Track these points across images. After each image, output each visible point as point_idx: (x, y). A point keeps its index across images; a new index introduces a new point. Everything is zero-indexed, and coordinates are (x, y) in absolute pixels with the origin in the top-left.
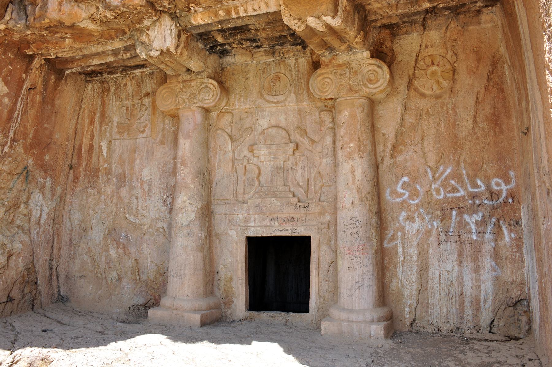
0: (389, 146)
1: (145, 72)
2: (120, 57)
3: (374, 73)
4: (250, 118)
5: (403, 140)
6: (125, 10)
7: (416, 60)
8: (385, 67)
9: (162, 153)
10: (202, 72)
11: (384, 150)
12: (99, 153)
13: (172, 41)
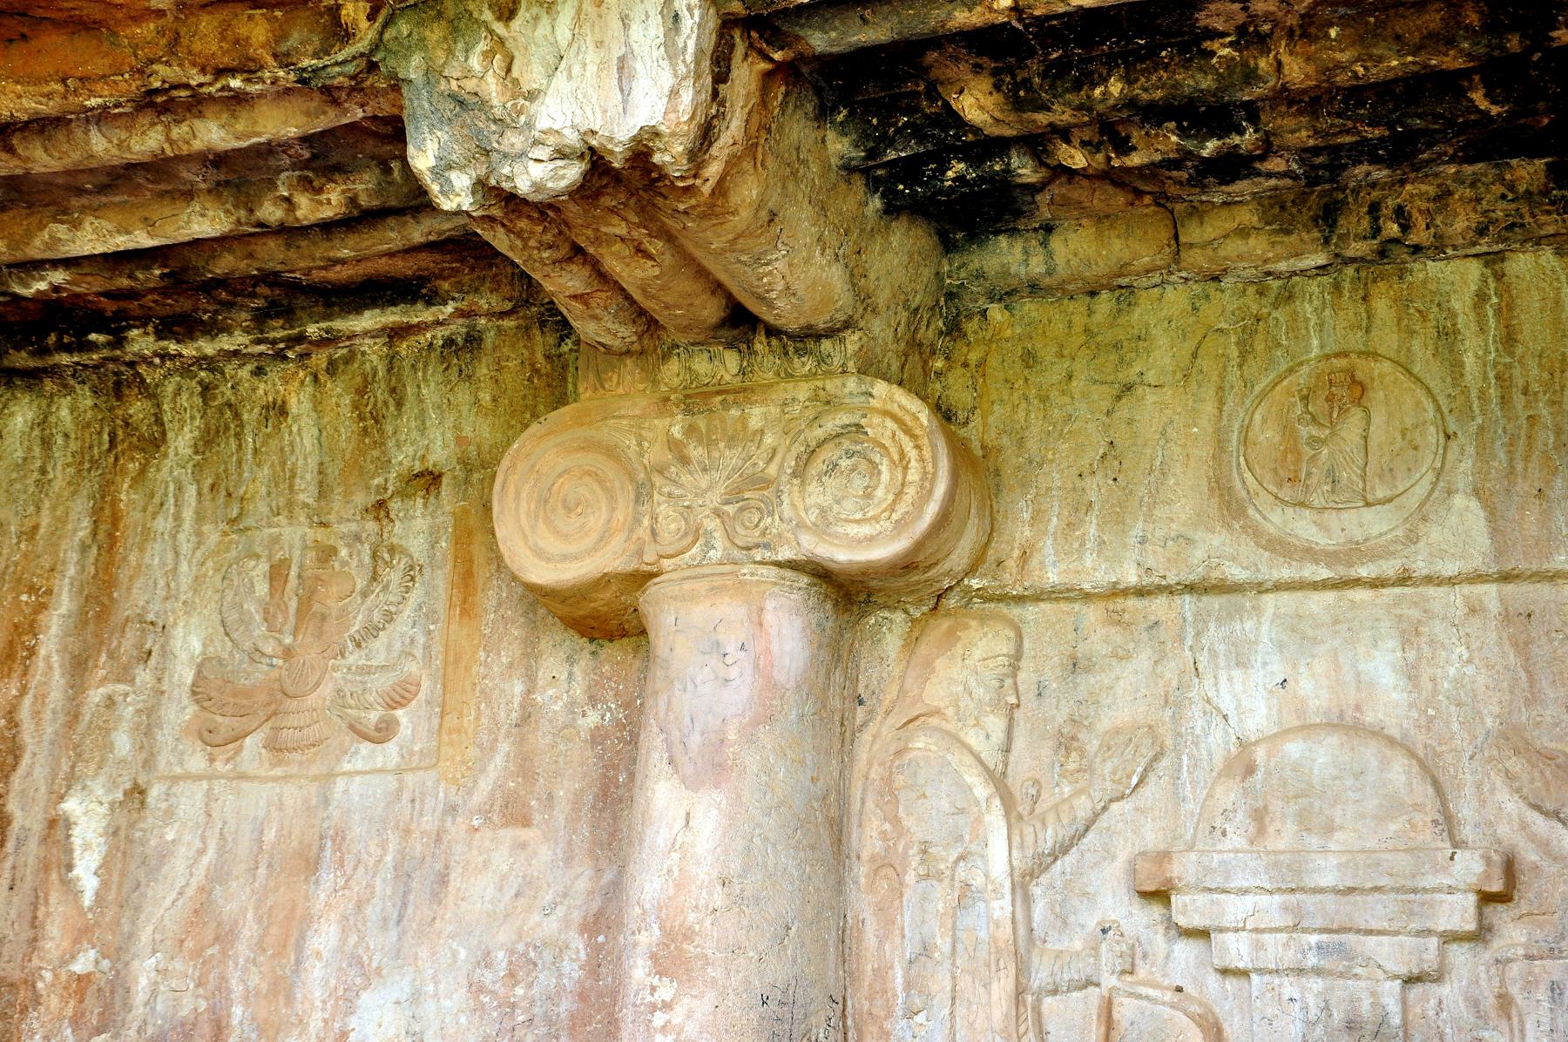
1: (420, 328)
2: (271, 212)
4: (1143, 659)
9: (512, 886)
12: (45, 867)
13: (674, 93)
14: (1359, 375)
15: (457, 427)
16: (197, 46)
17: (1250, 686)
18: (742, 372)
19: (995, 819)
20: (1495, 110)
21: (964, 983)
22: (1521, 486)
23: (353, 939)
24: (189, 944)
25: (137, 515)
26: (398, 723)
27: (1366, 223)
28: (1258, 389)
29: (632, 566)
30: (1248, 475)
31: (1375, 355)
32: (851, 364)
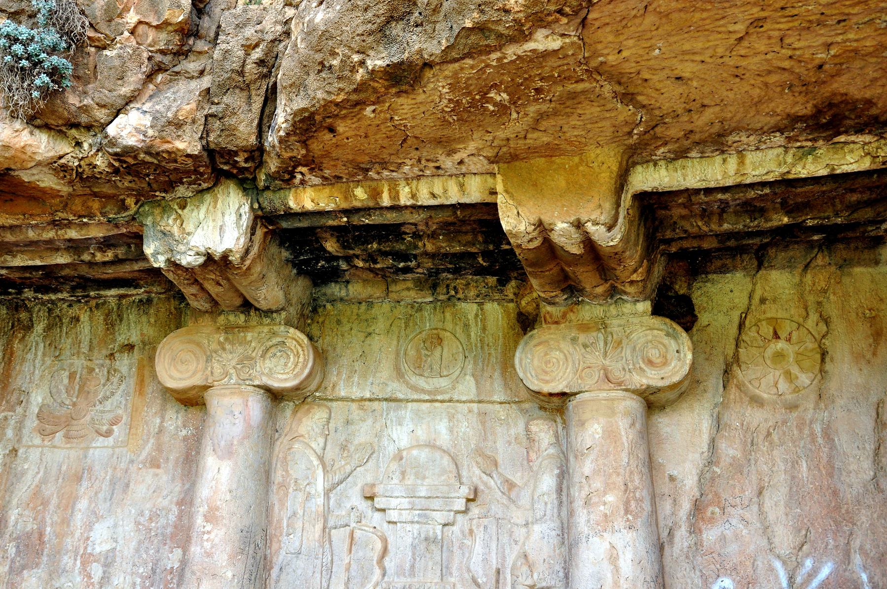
0: (686, 506)
1: (131, 296)
2: (86, 257)
4: (370, 421)
5: (717, 495)
6: (148, 159)
7: (741, 326)
9: (153, 489)
10: (276, 311)
13: (238, 239)
16: (74, 208)
17: (403, 431)
18: (246, 321)
19: (320, 472)
22: (486, 374)
23: (93, 505)
24: (31, 505)
25: (20, 353)
27: (445, 290)
29: (204, 383)
31: (445, 330)
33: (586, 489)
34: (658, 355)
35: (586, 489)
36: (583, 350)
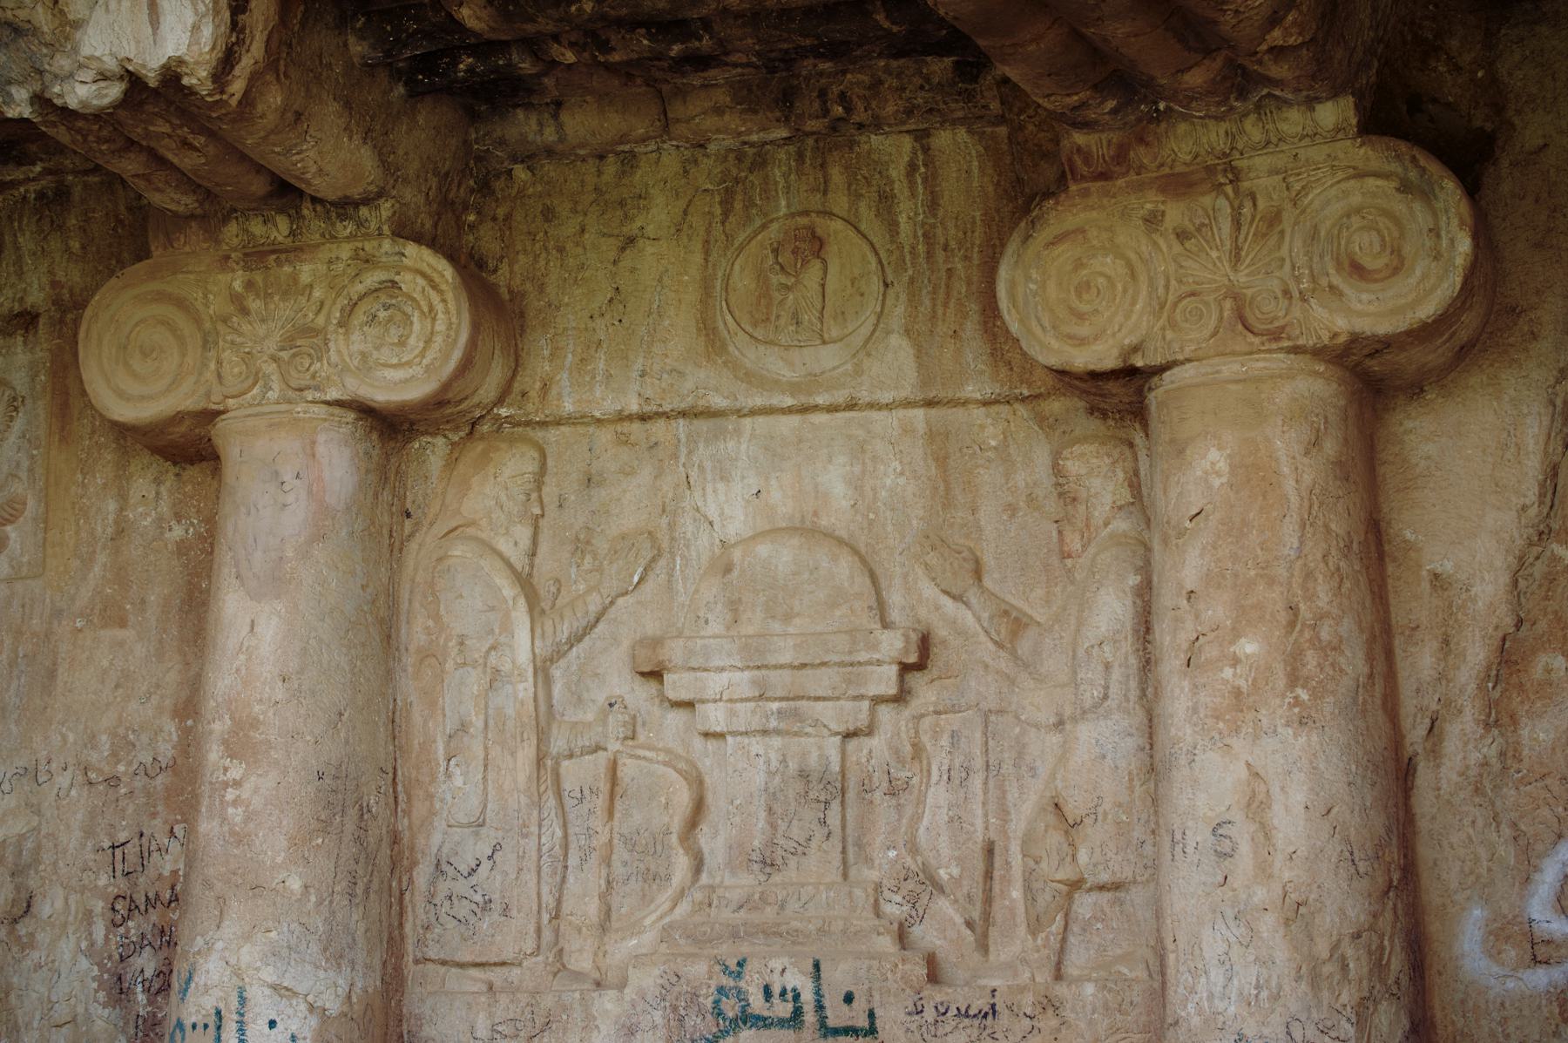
0: (1476, 653)
3: (1383, 222)
4: (646, 474)
8: (1450, 190)
11: (1442, 677)
13: (196, 28)
14: (819, 232)
15: (51, 272)
17: (734, 495)
18: (292, 233)
20: (895, 29)
21: (495, 752)
22: (942, 329)
26: (8, 538)
27: (817, 105)
28: (737, 244)
30: (729, 318)
32: (386, 228)
33: (1189, 625)
34: (1377, 248)
35: (1189, 625)
36: (1177, 248)
